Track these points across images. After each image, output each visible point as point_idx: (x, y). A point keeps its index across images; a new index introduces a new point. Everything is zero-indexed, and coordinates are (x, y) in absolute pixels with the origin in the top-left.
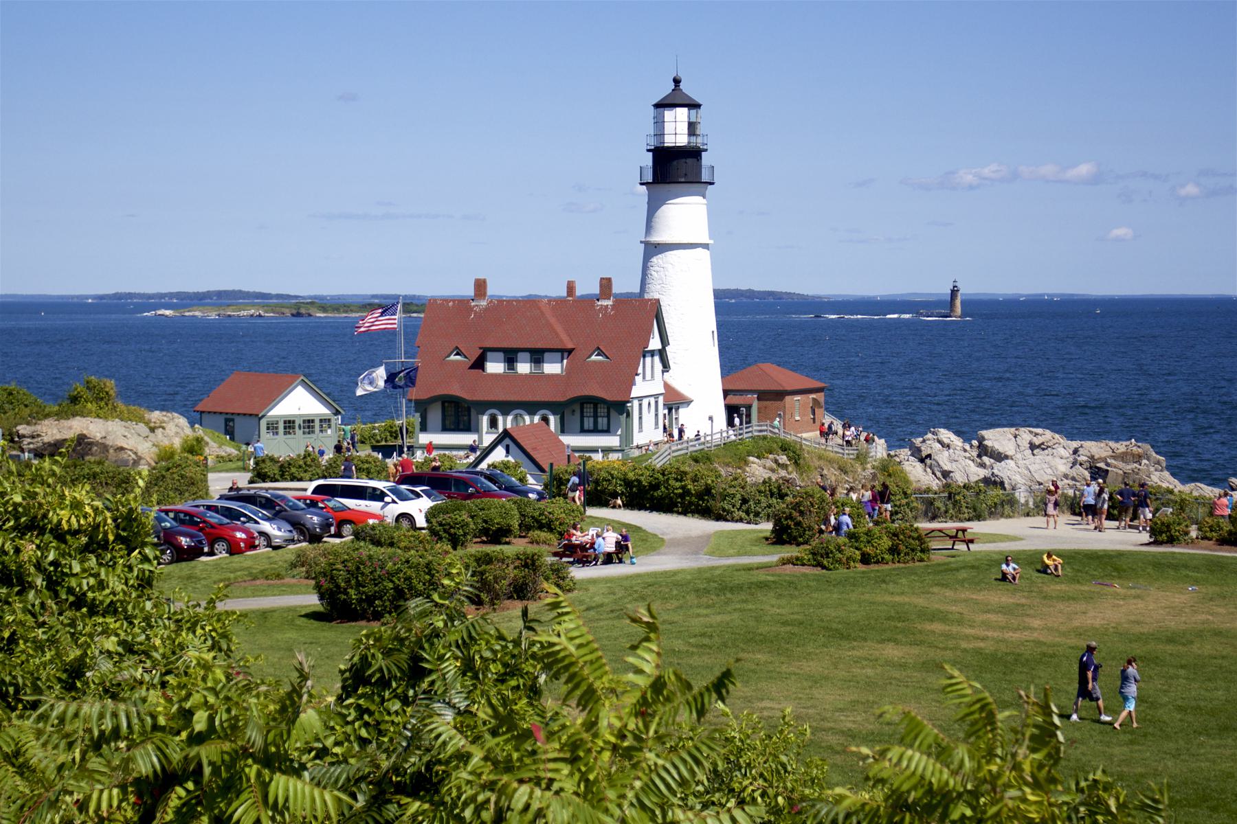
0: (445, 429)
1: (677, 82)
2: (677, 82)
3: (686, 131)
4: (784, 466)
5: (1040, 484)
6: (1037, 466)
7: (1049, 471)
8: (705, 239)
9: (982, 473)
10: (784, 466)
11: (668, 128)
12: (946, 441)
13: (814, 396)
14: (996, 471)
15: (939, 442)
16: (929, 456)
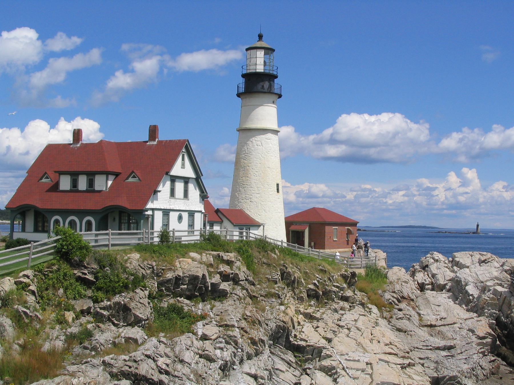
0: (36, 230)
1: (260, 37)
2: (260, 37)
3: (263, 63)
4: (229, 263)
5: (482, 282)
6: (482, 272)
7: (488, 275)
8: (275, 127)
9: (452, 275)
10: (229, 263)
12: (436, 258)
13: (349, 228)
14: (458, 274)
15: (433, 258)
16: (427, 266)
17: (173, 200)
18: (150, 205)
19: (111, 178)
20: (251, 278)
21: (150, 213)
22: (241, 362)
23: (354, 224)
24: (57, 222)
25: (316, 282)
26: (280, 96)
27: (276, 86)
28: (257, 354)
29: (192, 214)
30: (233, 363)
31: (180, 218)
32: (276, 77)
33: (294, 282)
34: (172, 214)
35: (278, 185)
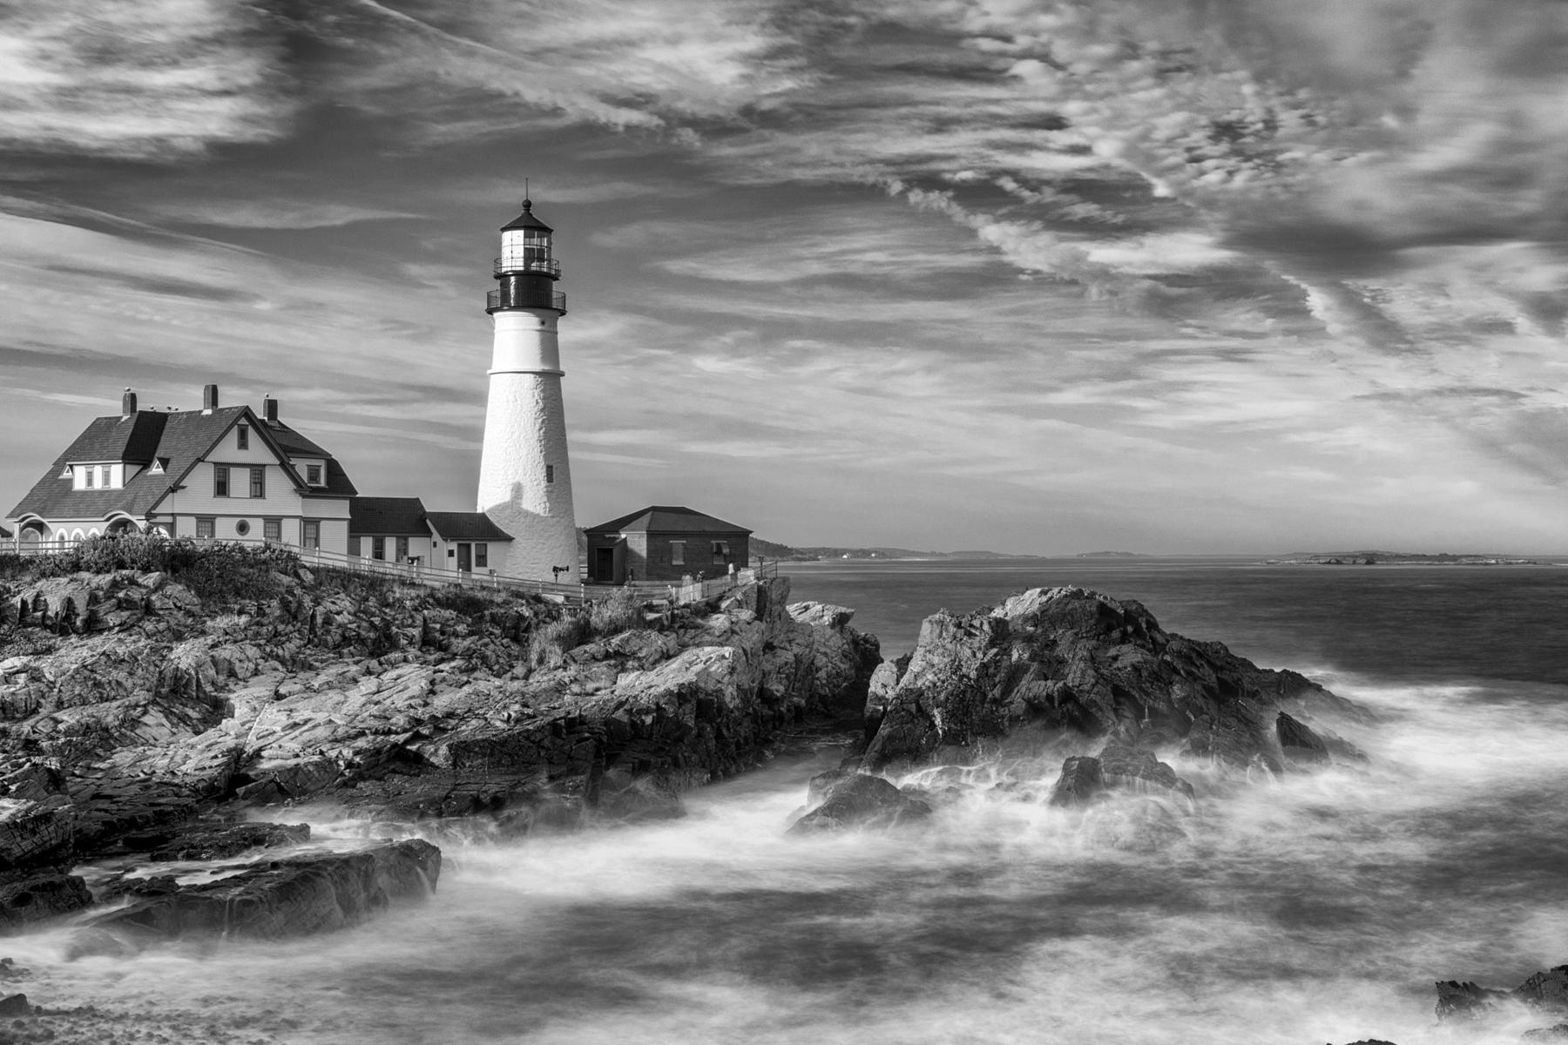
1: (528, 205)
11: (506, 253)
17: (222, 500)
18: (164, 508)
19: (138, 468)
20: (197, 609)
21: (170, 519)
22: (60, 705)
23: (745, 534)
24: (62, 537)
25: (376, 620)
26: (563, 313)
27: (554, 295)
28: (103, 699)
29: (273, 522)
30: (39, 704)
31: (243, 528)
32: (556, 278)
33: (313, 617)
34: (218, 521)
35: (549, 469)
